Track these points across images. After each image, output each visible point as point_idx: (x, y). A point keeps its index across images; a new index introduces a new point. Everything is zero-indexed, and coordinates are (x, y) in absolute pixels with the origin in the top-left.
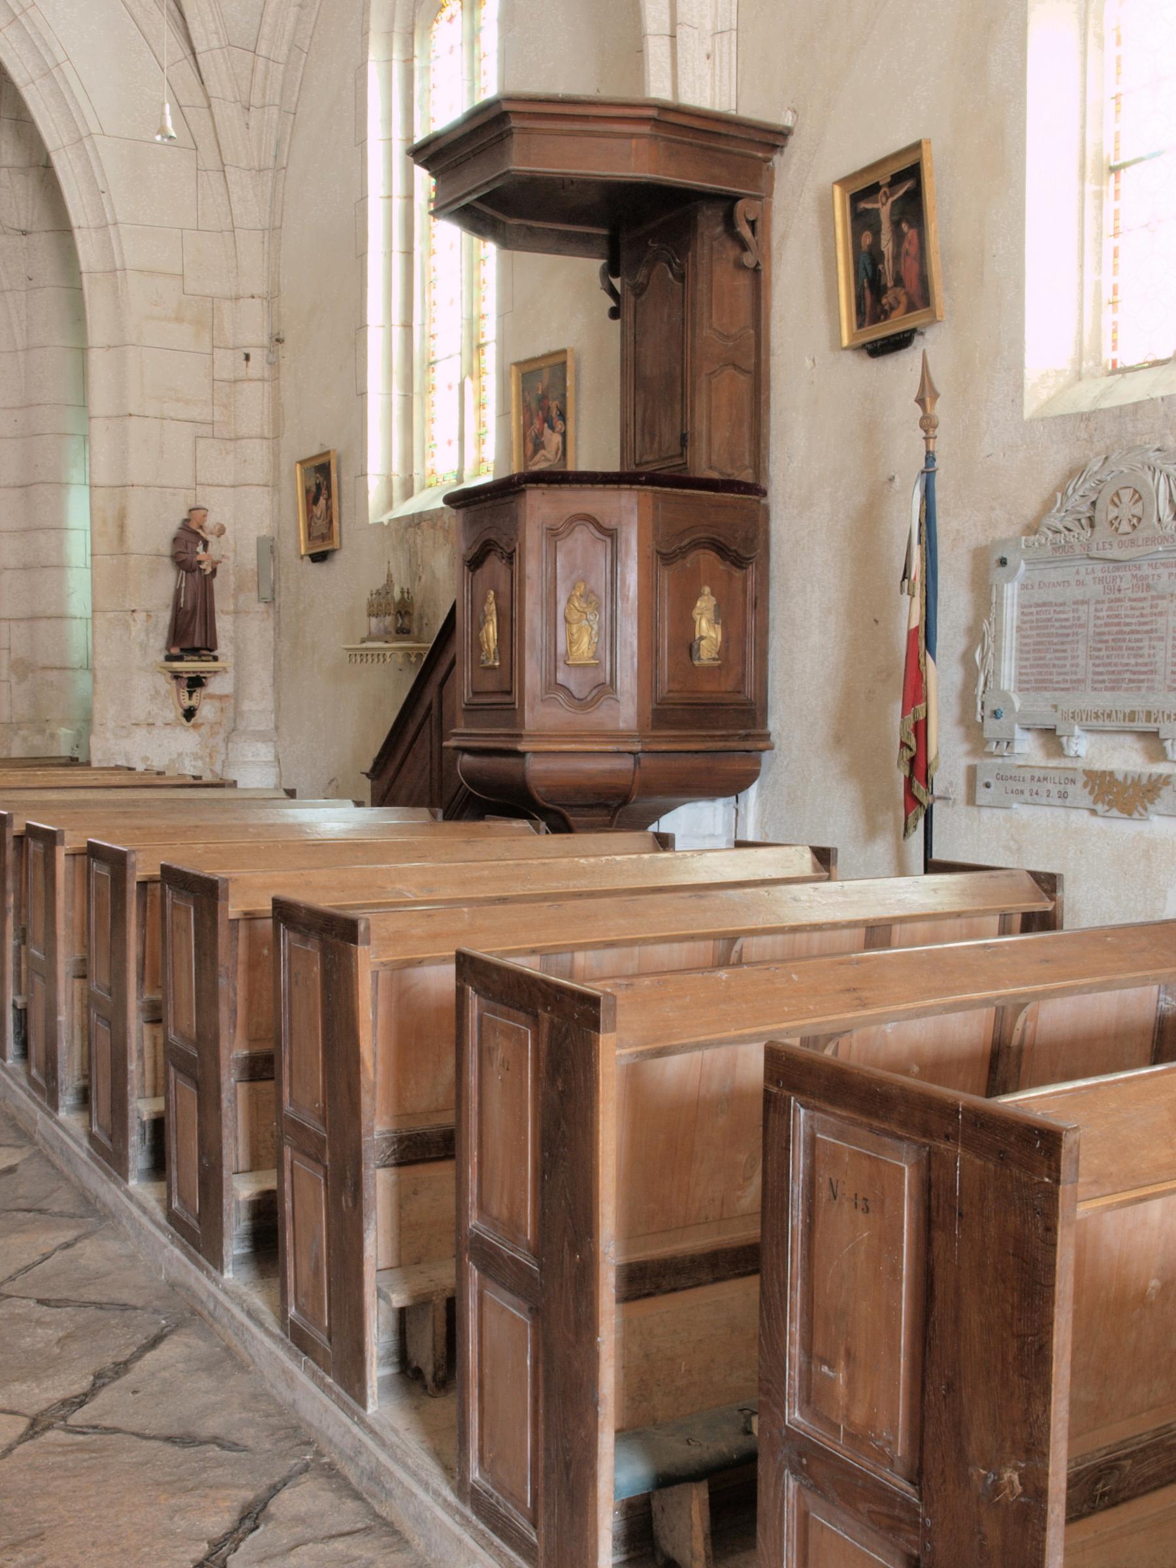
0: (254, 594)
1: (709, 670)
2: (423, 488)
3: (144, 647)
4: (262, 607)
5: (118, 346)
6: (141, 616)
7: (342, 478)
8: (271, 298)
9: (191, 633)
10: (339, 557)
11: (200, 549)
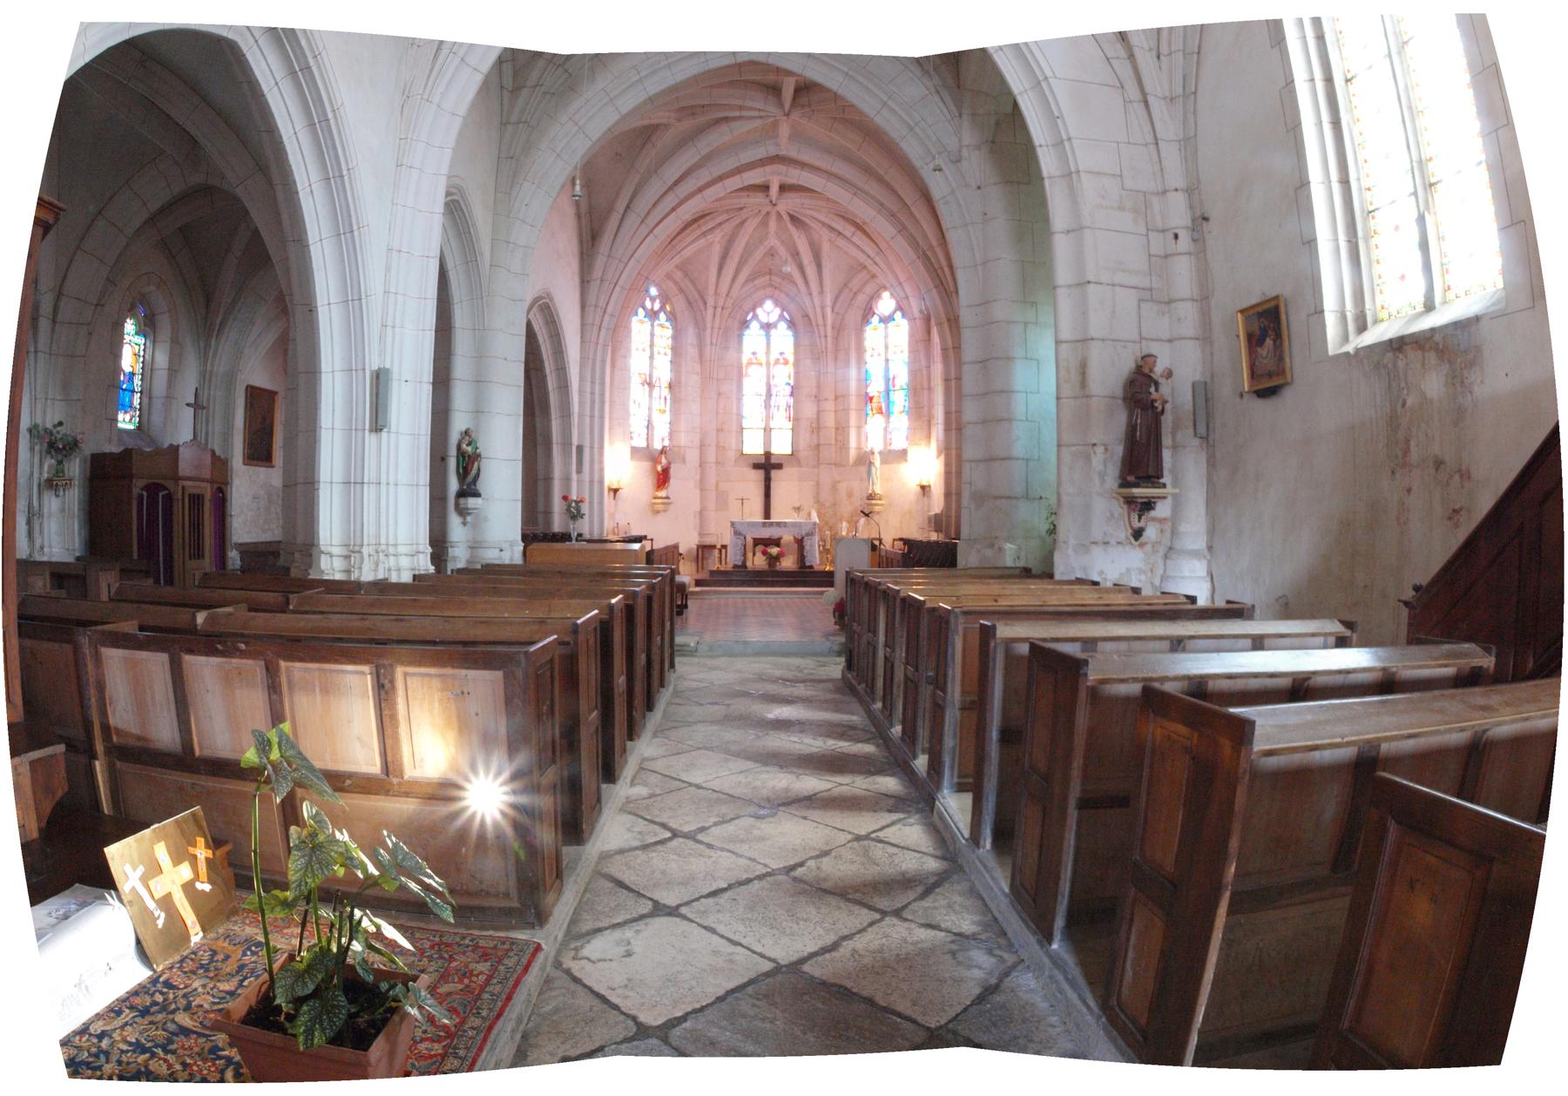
0: (1191, 430)
2: (1376, 322)
3: (1102, 476)
4: (1196, 442)
5: (1076, 230)
6: (1100, 449)
7: (1295, 321)
8: (1192, 191)
9: (1141, 464)
10: (1288, 395)
11: (1152, 390)
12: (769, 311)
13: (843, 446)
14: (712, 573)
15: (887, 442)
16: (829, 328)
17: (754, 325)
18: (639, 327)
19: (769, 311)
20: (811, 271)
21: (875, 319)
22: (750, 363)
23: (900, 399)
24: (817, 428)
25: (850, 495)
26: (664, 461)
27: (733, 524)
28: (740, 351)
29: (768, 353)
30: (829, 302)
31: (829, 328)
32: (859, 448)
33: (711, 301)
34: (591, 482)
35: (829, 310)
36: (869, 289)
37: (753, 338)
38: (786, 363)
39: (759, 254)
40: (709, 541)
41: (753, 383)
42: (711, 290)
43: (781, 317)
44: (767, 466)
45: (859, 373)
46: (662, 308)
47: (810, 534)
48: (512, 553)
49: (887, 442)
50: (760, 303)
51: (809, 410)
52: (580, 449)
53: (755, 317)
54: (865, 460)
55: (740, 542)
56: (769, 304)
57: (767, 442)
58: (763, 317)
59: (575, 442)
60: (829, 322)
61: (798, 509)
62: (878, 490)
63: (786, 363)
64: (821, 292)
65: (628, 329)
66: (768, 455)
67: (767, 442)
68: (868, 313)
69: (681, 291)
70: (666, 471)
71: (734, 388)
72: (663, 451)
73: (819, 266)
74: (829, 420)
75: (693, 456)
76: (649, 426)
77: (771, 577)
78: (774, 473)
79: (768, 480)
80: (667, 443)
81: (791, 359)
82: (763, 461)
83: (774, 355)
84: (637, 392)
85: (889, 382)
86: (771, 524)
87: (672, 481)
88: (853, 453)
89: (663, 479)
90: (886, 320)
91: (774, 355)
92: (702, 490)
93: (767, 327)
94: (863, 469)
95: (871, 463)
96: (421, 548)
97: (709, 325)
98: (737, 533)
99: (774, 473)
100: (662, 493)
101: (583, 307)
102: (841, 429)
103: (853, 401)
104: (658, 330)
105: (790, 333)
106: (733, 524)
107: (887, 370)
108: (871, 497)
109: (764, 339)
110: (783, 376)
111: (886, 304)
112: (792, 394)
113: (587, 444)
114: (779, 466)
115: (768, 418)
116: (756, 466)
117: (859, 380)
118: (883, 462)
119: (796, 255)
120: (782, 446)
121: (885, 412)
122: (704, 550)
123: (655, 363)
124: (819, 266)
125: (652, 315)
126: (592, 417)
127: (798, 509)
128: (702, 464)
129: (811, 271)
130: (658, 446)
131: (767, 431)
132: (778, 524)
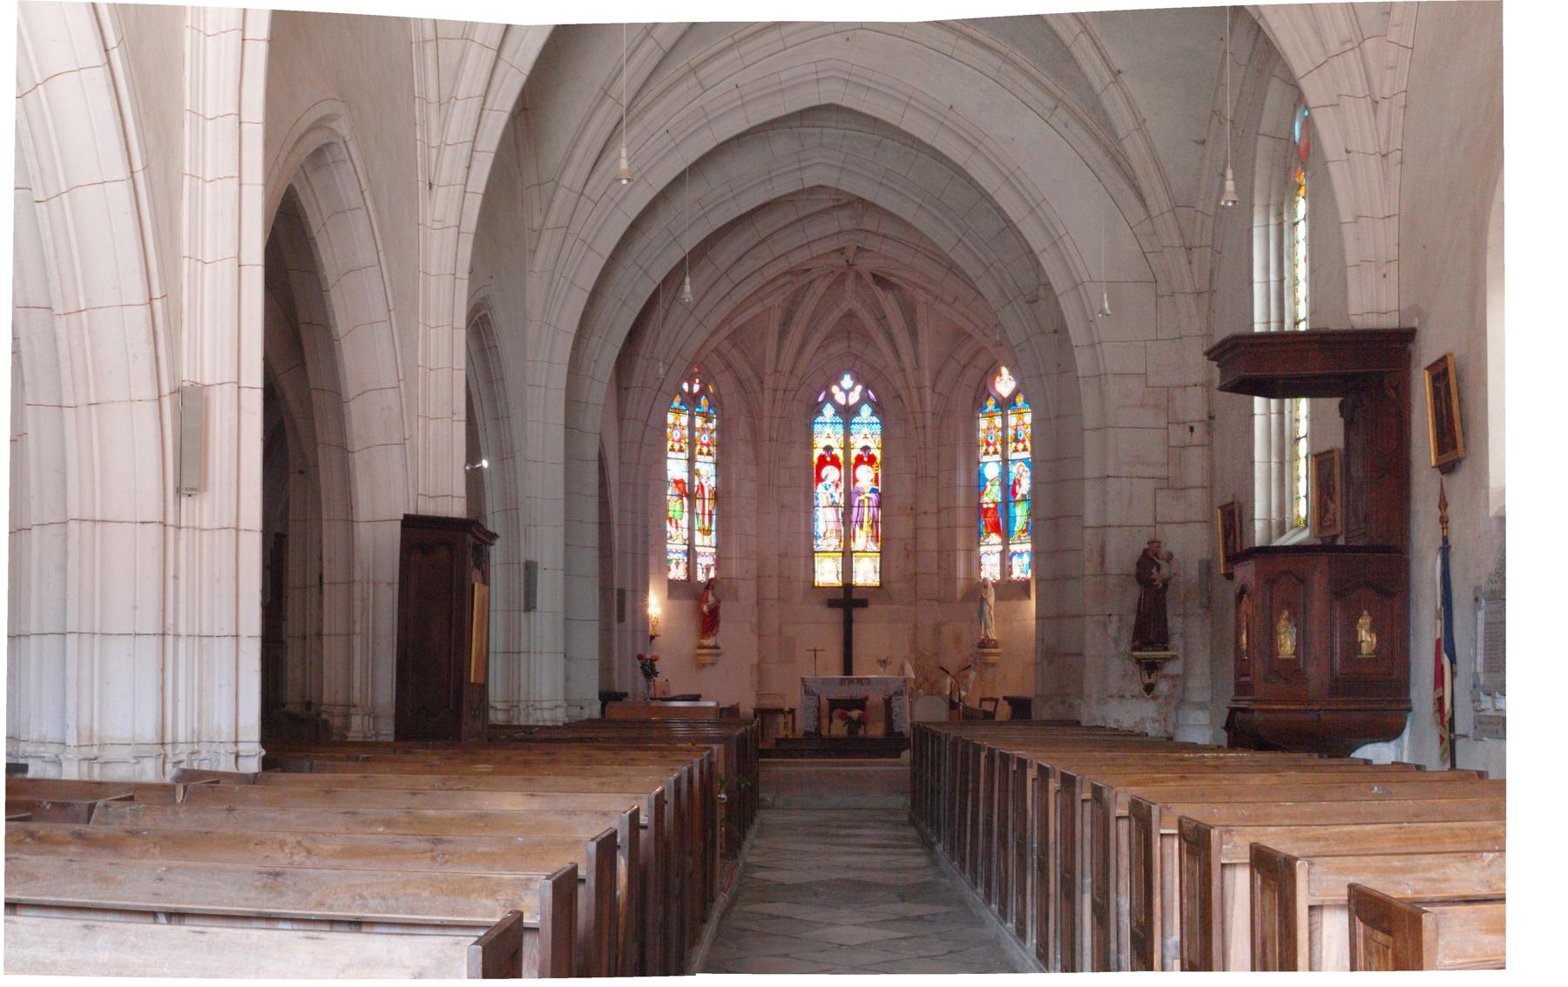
1: (1368, 660)
3: (1116, 641)
6: (1115, 619)
9: (1150, 633)
12: (847, 389)
13: (950, 578)
14: (778, 741)
15: (1006, 568)
16: (929, 415)
17: (829, 410)
18: (677, 421)
19: (847, 389)
20: (903, 340)
21: (991, 405)
22: (823, 462)
23: (1020, 513)
24: (913, 550)
25: (957, 641)
26: (711, 598)
27: (803, 680)
28: (810, 446)
29: (847, 448)
30: (928, 383)
31: (929, 415)
32: (969, 579)
33: (769, 382)
34: (634, 632)
35: (928, 392)
36: (982, 361)
37: (827, 435)
38: (872, 460)
39: (835, 315)
40: (768, 703)
41: (828, 491)
42: (769, 369)
43: (864, 399)
44: (848, 599)
45: (969, 476)
46: (703, 391)
47: (899, 693)
48: (594, 711)
49: (1006, 568)
50: (837, 380)
51: (903, 527)
52: (621, 593)
53: (830, 398)
54: (977, 590)
55: (813, 703)
56: (847, 381)
57: (847, 570)
58: (840, 398)
59: (616, 587)
60: (929, 409)
61: (883, 663)
62: (993, 636)
63: (872, 460)
64: (917, 368)
65: (665, 425)
66: (848, 587)
67: (847, 570)
68: (983, 391)
69: (729, 366)
70: (714, 611)
71: (802, 497)
72: (710, 584)
73: (913, 333)
74: (930, 542)
75: (747, 591)
76: (691, 553)
77: (853, 746)
78: (857, 613)
79: (848, 624)
80: (712, 575)
81: (877, 454)
82: (841, 596)
83: (854, 453)
84: (676, 507)
85: (1009, 489)
86: (851, 681)
87: (722, 625)
88: (961, 585)
89: (709, 623)
90: (1006, 404)
91: (854, 453)
92: (760, 636)
93: (847, 414)
94: (973, 606)
95: (983, 600)
96: (559, 703)
97: (766, 413)
98: (807, 692)
99: (857, 613)
100: (709, 642)
101: (621, 418)
102: (946, 552)
103: (961, 516)
104: (699, 422)
105: (875, 419)
106: (803, 680)
107: (1005, 472)
108: (985, 643)
109: (840, 429)
110: (865, 475)
111: (1005, 384)
112: (879, 506)
113: (629, 587)
114: (863, 603)
115: (849, 537)
116: (832, 604)
117: (969, 486)
118: (999, 598)
119: (882, 319)
120: (866, 573)
121: (1005, 533)
122: (764, 713)
123: (697, 466)
124: (913, 333)
125: (691, 401)
126: (634, 554)
127: (883, 663)
128: (760, 601)
129: (903, 340)
130: (701, 577)
131: (847, 555)
132: (860, 680)
